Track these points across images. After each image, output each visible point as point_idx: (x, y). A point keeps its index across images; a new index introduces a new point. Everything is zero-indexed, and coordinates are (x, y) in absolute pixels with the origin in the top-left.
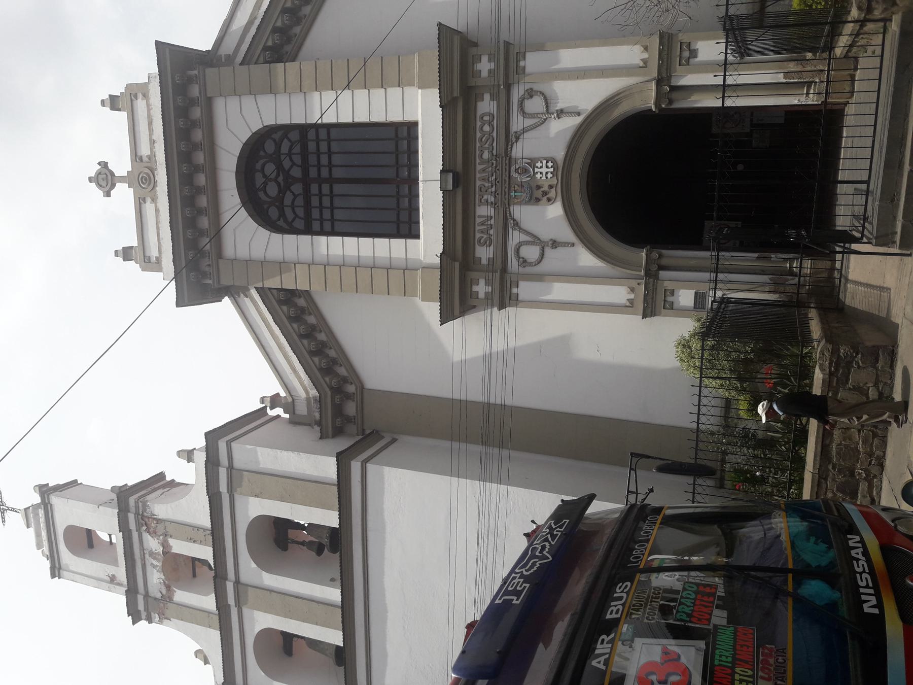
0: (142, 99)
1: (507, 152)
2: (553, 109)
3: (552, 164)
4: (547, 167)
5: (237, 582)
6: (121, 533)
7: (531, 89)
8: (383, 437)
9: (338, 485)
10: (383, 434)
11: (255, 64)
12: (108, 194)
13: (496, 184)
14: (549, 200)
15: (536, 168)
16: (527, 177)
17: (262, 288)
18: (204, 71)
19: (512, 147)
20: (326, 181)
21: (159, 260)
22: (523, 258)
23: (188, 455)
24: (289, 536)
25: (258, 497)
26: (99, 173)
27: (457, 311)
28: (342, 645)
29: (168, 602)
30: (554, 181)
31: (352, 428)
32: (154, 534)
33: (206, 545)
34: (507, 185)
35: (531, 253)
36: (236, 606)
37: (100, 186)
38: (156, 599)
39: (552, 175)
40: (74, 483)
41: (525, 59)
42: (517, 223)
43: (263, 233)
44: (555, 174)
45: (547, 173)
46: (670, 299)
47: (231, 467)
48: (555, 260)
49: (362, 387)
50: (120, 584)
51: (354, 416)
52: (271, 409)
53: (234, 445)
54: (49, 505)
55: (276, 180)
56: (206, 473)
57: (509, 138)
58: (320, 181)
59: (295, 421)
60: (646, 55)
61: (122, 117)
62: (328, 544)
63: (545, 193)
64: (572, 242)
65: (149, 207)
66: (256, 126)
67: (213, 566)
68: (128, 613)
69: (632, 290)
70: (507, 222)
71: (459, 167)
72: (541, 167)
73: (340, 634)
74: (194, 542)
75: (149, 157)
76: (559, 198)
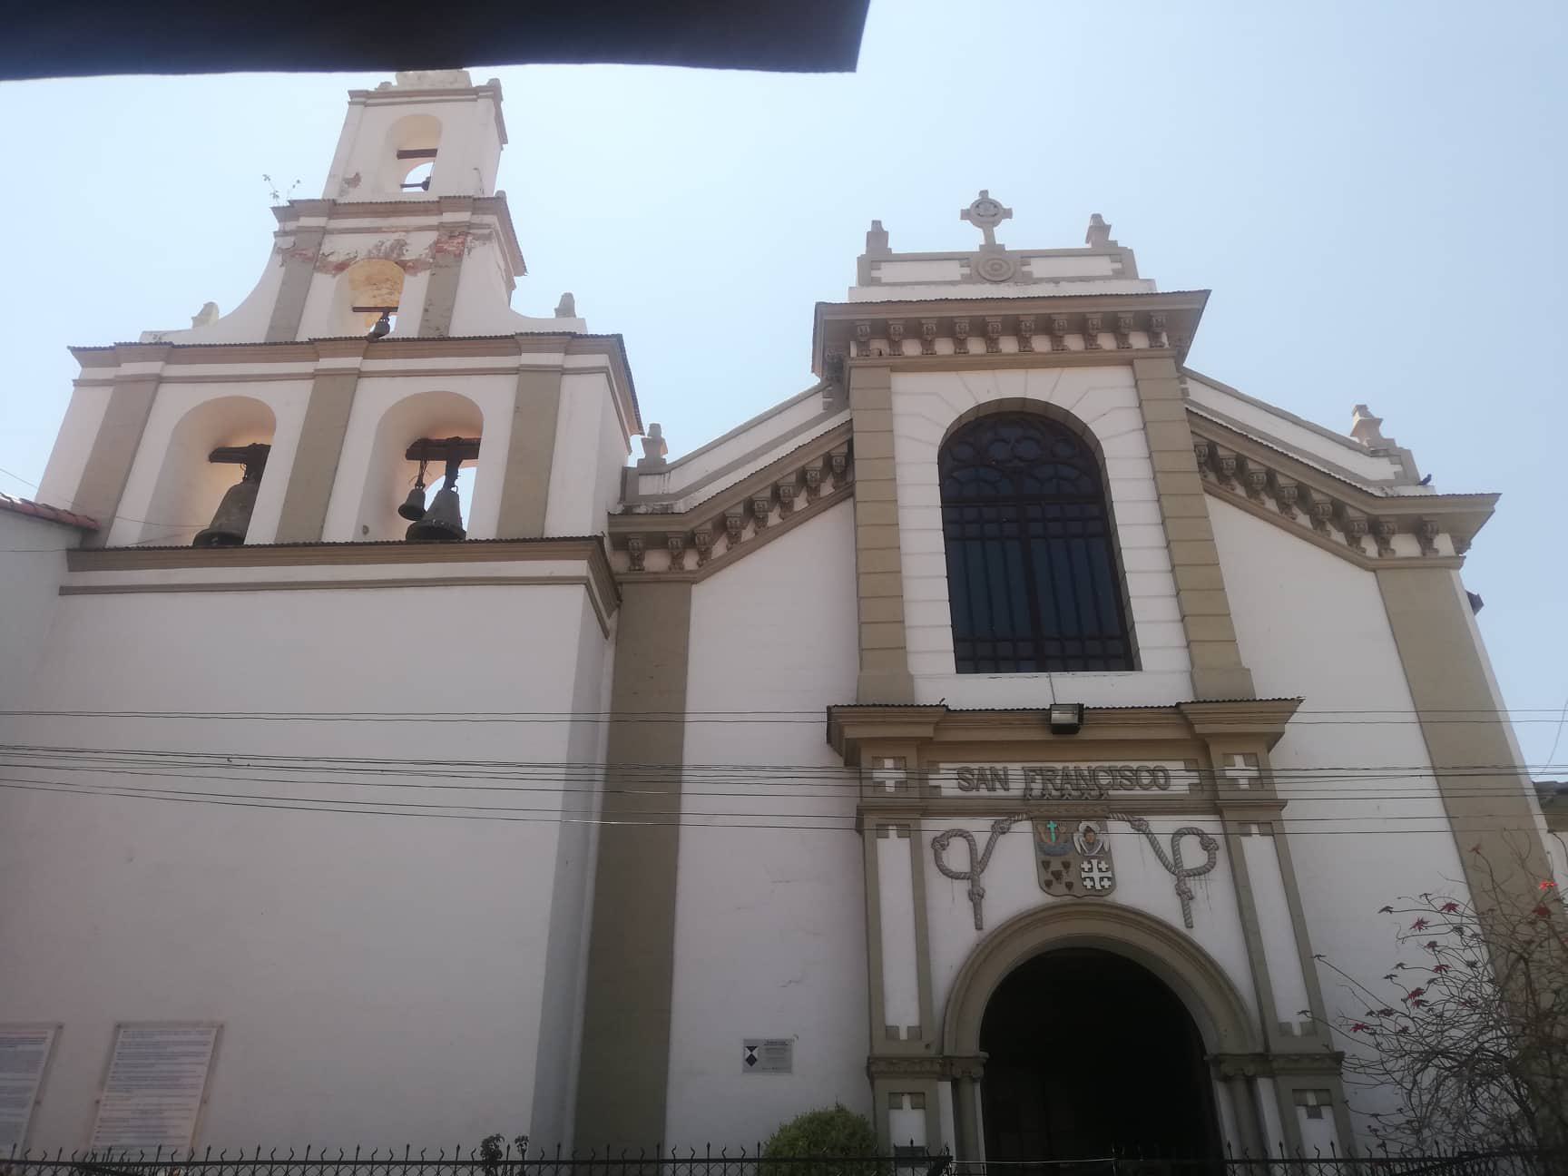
0: (1113, 270)
1: (1120, 813)
2: (1192, 884)
3: (1107, 887)
4: (1102, 879)
6: (437, 199)
7: (1218, 848)
8: (609, 616)
9: (542, 538)
10: (615, 614)
11: (1192, 432)
12: (966, 215)
13: (1063, 796)
14: (1047, 885)
15: (1096, 861)
16: (1081, 846)
17: (850, 430)
18: (1169, 357)
19: (1124, 820)
21: (876, 282)
22: (948, 845)
23: (566, 307)
24: (431, 462)
25: (515, 412)
26: (996, 205)
27: (850, 733)
28: (248, 541)
29: (315, 266)
31: (619, 562)
32: (437, 248)
33: (422, 327)
34: (1064, 813)
35: (957, 856)
36: (316, 370)
37: (977, 205)
38: (320, 245)
39: (1089, 887)
40: (503, 138)
41: (1262, 834)
42: (1004, 833)
43: (937, 436)
44: (1095, 893)
45: (1092, 879)
46: (906, 1101)
48: (949, 902)
49: (694, 579)
50: (342, 192)
51: (643, 570)
52: (643, 440)
53: (603, 377)
54: (475, 97)
56: (554, 334)
57: (1135, 813)
59: (627, 477)
60: (1297, 1031)
61: (1081, 243)
62: (428, 524)
63: (1057, 875)
64: (984, 927)
66: (1099, 429)
67: (384, 337)
68: (295, 201)
69: (916, 1033)
70: (1004, 814)
71: (1084, 734)
72: (1100, 870)
73: (268, 539)
74: (426, 310)
75: (1030, 274)
76: (1049, 900)
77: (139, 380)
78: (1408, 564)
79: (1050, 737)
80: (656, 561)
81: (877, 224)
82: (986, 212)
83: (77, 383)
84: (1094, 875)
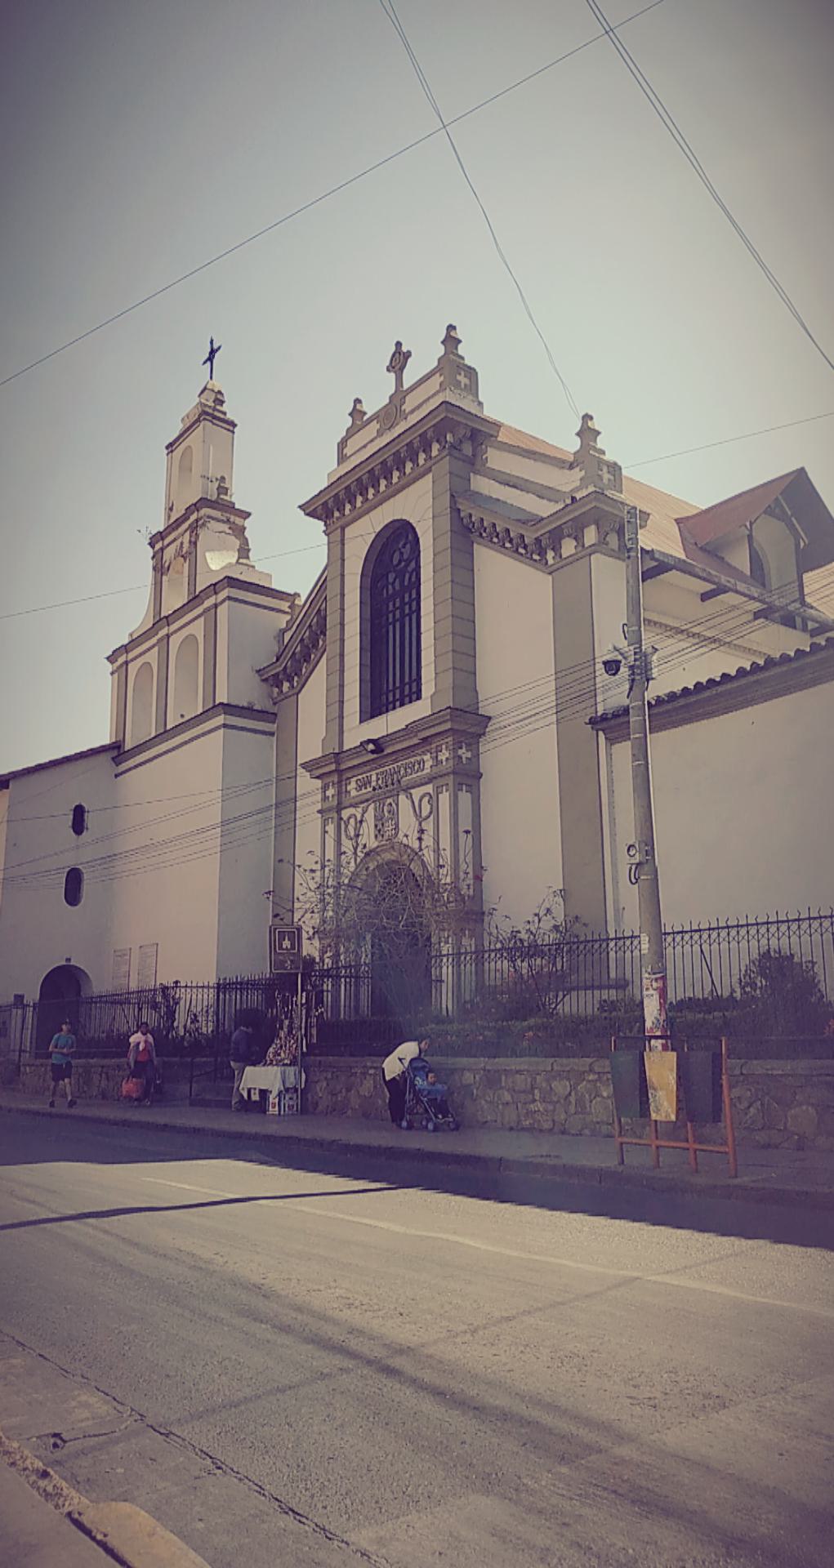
5: (168, 636)
8: (274, 722)
10: (277, 721)
11: (455, 511)
14: (376, 836)
20: (403, 611)
30: (386, 837)
32: (190, 542)
47: (216, 606)
50: (169, 517)
55: (400, 562)
57: (407, 790)
58: (403, 603)
63: (379, 831)
65: (375, 426)
71: (385, 753)
77: (121, 665)
78: (574, 559)
79: (375, 756)
80: (286, 685)
81: (358, 401)
82: (399, 360)
83: (112, 673)
84: (389, 827)
